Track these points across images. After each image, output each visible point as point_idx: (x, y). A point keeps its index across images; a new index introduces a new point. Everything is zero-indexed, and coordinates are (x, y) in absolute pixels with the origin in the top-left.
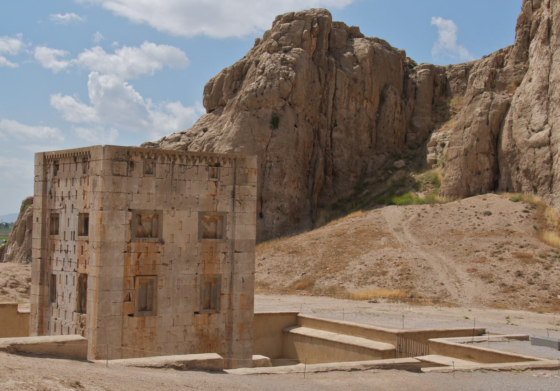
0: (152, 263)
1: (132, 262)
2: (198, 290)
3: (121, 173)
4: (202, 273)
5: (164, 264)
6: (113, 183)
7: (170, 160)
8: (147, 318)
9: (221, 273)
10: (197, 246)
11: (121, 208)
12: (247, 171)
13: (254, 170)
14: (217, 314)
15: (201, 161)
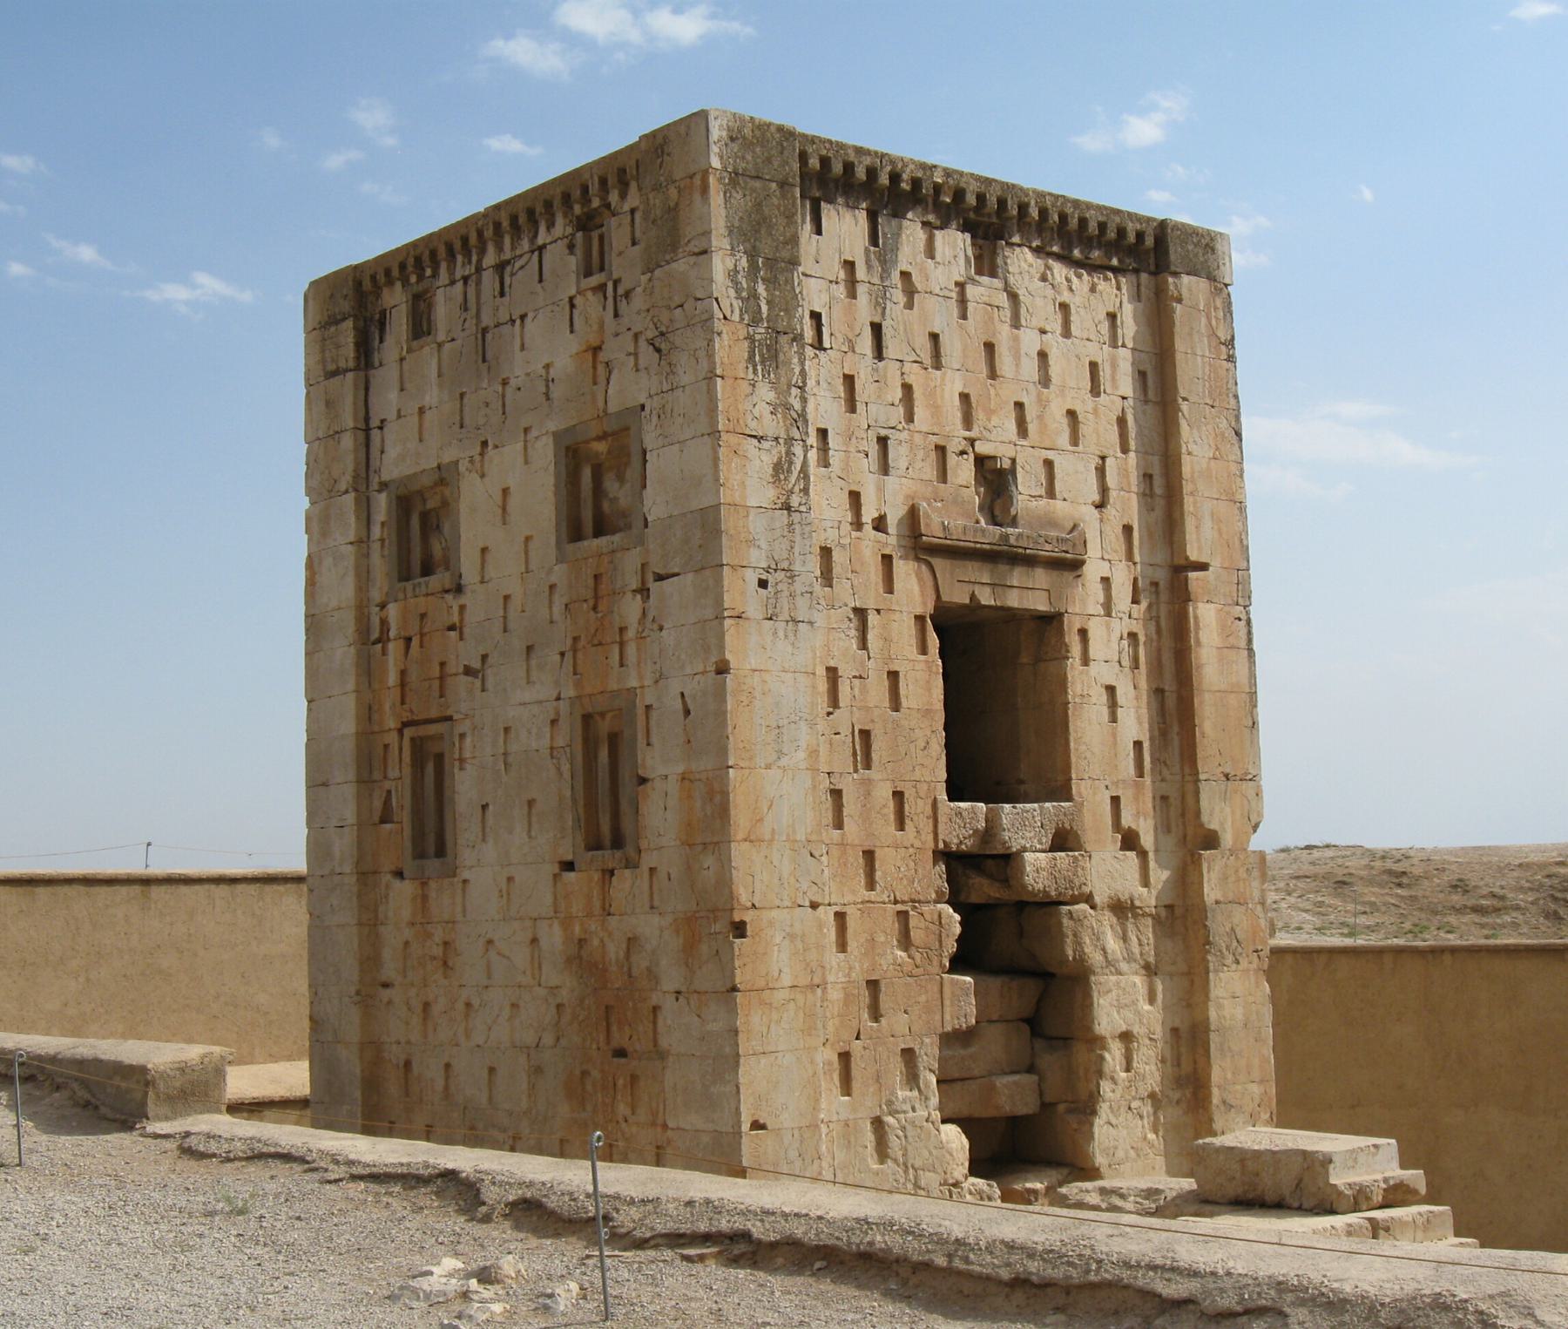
0: (436, 672)
1: (392, 678)
2: (566, 768)
3: (342, 364)
4: (572, 693)
5: (468, 671)
6: (328, 404)
7: (470, 262)
8: (433, 884)
9: (633, 683)
10: (553, 579)
11: (343, 488)
12: (673, 192)
13: (697, 181)
14: (627, 872)
15: (551, 225)
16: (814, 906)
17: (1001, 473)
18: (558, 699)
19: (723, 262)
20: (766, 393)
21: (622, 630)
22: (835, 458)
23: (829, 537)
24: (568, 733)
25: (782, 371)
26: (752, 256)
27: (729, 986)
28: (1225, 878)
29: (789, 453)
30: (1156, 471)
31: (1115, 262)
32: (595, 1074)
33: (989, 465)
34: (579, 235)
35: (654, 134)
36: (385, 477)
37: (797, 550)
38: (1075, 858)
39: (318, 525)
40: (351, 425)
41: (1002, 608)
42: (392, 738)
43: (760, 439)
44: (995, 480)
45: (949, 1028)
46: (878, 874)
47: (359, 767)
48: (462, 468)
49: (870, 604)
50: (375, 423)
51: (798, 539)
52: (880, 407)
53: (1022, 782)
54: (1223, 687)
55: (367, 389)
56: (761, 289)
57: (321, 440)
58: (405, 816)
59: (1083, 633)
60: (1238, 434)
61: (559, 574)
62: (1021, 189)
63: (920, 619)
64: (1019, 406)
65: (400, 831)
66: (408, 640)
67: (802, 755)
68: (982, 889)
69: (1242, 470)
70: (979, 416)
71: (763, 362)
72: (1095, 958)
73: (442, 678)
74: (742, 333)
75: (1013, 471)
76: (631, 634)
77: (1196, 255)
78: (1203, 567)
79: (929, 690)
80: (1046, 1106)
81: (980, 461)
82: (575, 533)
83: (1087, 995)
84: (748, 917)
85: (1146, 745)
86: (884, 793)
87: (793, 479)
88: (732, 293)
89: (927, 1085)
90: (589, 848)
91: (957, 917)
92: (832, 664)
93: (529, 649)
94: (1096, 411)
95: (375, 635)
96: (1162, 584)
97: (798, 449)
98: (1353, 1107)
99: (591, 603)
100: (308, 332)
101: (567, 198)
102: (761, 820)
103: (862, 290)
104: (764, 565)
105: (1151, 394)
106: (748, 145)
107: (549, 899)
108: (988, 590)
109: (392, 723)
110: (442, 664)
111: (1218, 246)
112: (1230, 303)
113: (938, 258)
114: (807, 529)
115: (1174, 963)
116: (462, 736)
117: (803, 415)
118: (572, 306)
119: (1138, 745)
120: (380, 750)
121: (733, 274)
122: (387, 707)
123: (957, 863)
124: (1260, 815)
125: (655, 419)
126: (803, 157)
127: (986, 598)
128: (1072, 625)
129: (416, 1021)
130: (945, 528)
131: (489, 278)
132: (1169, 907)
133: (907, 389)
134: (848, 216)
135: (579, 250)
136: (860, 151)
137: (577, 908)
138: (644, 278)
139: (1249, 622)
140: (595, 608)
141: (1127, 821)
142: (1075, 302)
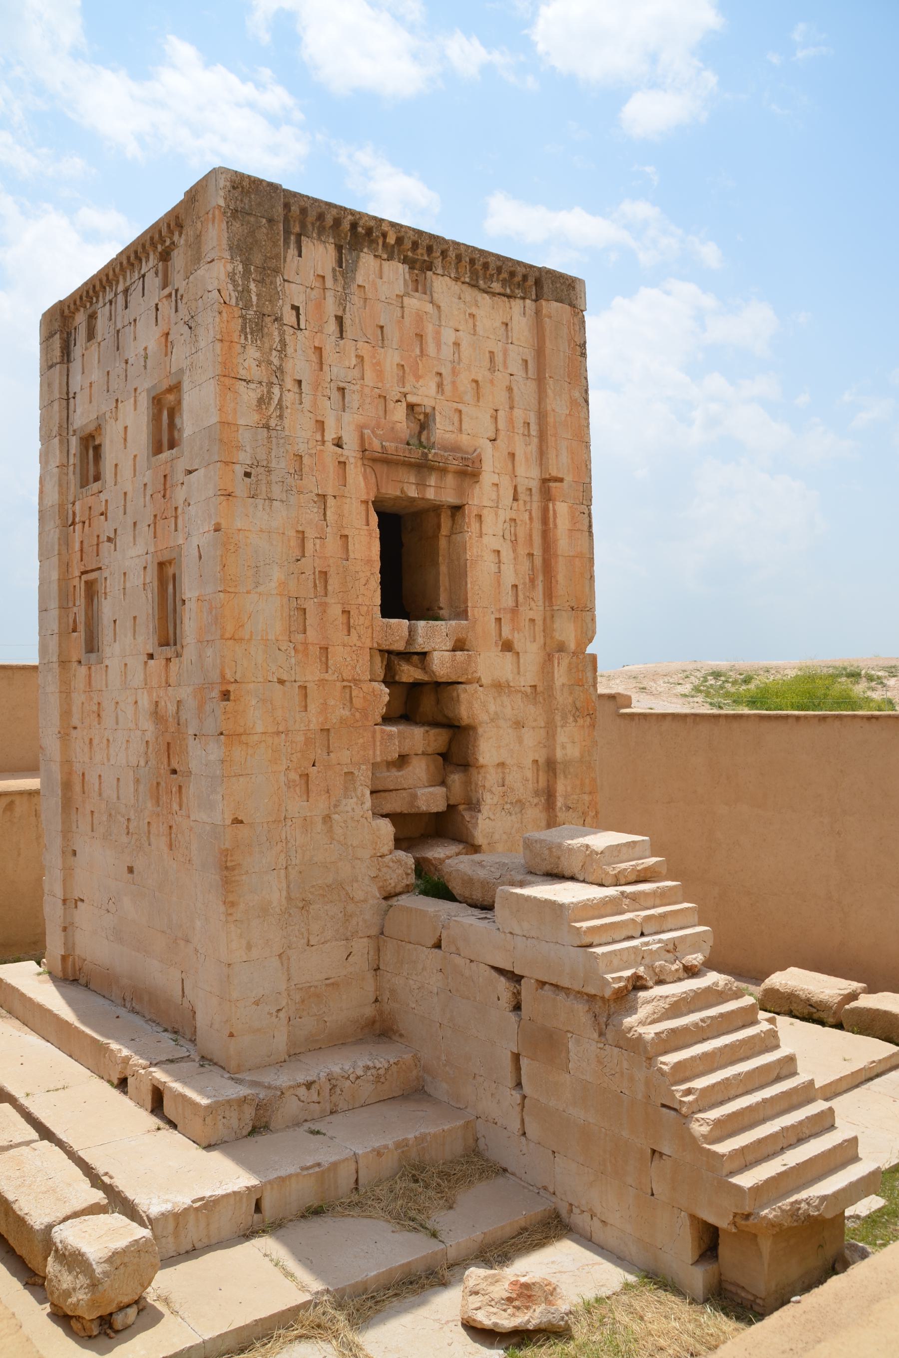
1: (77, 547)
2: (150, 596)
3: (55, 361)
5: (109, 540)
9: (181, 542)
10: (146, 480)
16: (281, 682)
17: (426, 415)
18: (147, 553)
19: (225, 267)
20: (253, 353)
21: (176, 508)
22: (307, 400)
23: (302, 448)
24: (152, 575)
25: (266, 340)
26: (246, 263)
27: (219, 732)
28: (570, 669)
29: (269, 392)
30: (533, 420)
31: (508, 291)
32: (163, 784)
33: (417, 409)
34: (160, 264)
35: (191, 189)
36: (75, 427)
37: (273, 454)
38: (469, 656)
39: (45, 457)
40: (58, 396)
41: (423, 499)
42: (76, 582)
43: (248, 382)
44: (421, 420)
45: (379, 759)
46: (330, 662)
47: (60, 600)
48: (107, 417)
49: (330, 492)
50: (71, 395)
51: (274, 447)
52: (340, 366)
53: (441, 608)
54: (571, 554)
55: (68, 375)
56: (252, 286)
57: (46, 406)
58: (81, 627)
59: (479, 517)
60: (587, 401)
61: (148, 477)
62: (443, 239)
63: (366, 502)
64: (440, 374)
65: (80, 636)
66: (84, 523)
67: (273, 585)
68: (409, 673)
69: (588, 424)
70: (410, 379)
71: (252, 333)
72: (483, 717)
73: (98, 545)
74: (237, 313)
75: (434, 414)
76: (180, 511)
77: (562, 291)
78: (561, 480)
79: (370, 548)
80: (451, 808)
81: (411, 407)
82: (157, 449)
83: (476, 740)
84: (231, 688)
85: (520, 587)
86: (335, 611)
87: (272, 408)
88: (231, 287)
89: (363, 795)
90: (161, 645)
91: (387, 690)
92: (300, 529)
93: (135, 524)
94: (492, 382)
95: (70, 522)
96: (534, 490)
97: (276, 390)
98: (669, 803)
99: (162, 493)
100: (41, 344)
101: (153, 244)
102: (242, 626)
103: (330, 294)
104: (249, 462)
105: (530, 375)
106: (246, 192)
107: (142, 677)
108: (414, 487)
109: (77, 574)
110: (98, 536)
111: (577, 286)
112: (584, 322)
113: (385, 279)
114: (282, 441)
115: (535, 720)
116: (106, 578)
117: (280, 369)
118: (157, 309)
119: (515, 586)
120: (72, 589)
121: (232, 276)
122: (75, 562)
123: (392, 658)
124: (594, 632)
125: (188, 371)
126: (287, 206)
127: (413, 492)
128: (470, 511)
129: (86, 749)
130: (382, 446)
131: (120, 299)
132: (535, 687)
133: (360, 358)
134: (321, 248)
135: (160, 274)
136: (329, 205)
137: (154, 683)
138: (184, 283)
139: (590, 515)
140: (164, 496)
141: (506, 632)
142: (480, 313)
